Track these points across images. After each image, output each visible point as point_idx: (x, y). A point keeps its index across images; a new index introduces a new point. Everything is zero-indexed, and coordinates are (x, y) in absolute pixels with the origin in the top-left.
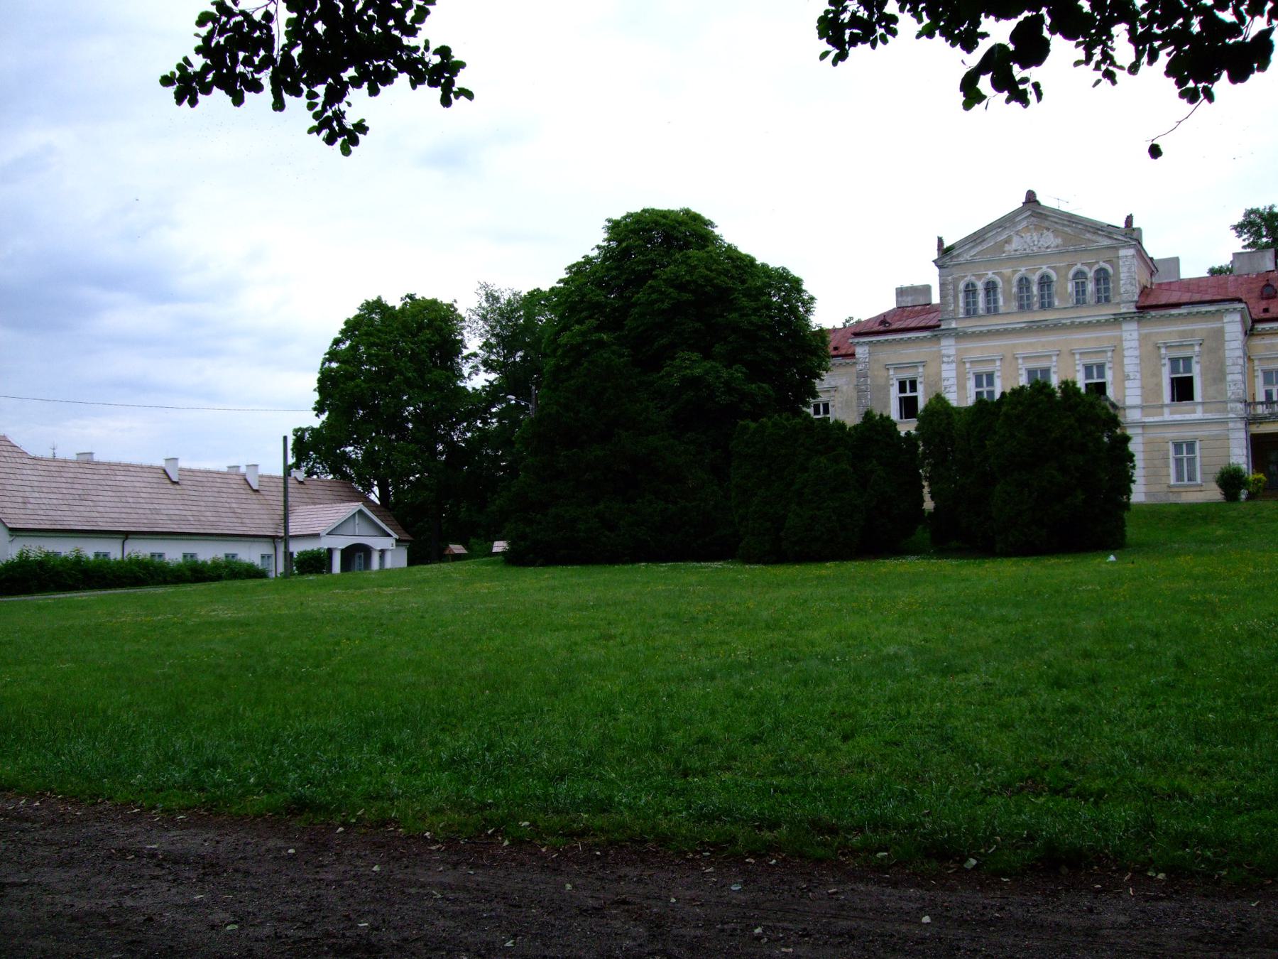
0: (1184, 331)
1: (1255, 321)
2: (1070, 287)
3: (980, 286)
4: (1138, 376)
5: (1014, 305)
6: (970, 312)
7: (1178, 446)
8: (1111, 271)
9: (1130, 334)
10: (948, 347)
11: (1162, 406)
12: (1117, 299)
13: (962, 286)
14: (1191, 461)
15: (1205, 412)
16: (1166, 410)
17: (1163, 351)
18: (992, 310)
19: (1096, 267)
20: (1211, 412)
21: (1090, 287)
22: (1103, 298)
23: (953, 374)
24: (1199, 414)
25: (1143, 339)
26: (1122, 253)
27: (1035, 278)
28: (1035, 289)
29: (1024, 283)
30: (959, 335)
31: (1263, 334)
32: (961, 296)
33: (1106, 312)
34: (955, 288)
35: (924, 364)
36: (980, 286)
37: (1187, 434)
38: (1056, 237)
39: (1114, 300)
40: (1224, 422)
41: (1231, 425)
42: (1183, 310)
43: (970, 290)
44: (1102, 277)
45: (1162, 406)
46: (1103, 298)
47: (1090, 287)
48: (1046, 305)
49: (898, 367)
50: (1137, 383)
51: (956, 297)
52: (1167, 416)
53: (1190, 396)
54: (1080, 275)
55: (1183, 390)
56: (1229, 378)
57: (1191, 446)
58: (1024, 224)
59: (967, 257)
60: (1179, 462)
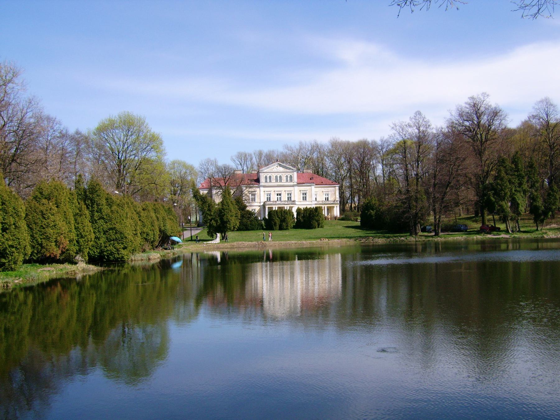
2: (285, 178)
6: (266, 181)
9: (297, 189)
10: (262, 189)
22: (291, 181)
24: (307, 203)
27: (279, 176)
30: (264, 186)
33: (292, 184)
42: (305, 184)
44: (291, 177)
46: (291, 181)
47: (289, 179)
48: (281, 181)
53: (306, 200)
54: (287, 176)
55: (305, 199)
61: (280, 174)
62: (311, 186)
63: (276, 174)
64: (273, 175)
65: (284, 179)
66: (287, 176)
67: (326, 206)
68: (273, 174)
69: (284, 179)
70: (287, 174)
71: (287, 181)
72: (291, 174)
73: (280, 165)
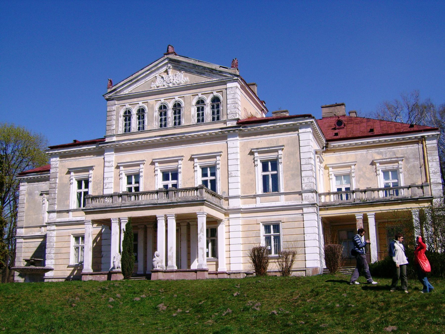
0: (271, 140)
1: (328, 141)
2: (194, 111)
3: (134, 112)
4: (239, 174)
5: (156, 125)
7: (267, 228)
8: (221, 99)
11: (255, 197)
12: (225, 118)
13: (122, 113)
14: (277, 238)
15: (286, 200)
16: (258, 199)
17: (256, 155)
18: (141, 129)
19: (211, 96)
20: (290, 200)
21: (208, 110)
23: (113, 174)
24: (282, 201)
25: (243, 146)
26: (229, 85)
27: (170, 105)
28: (170, 113)
29: (163, 109)
31: (334, 150)
32: (121, 119)
34: (118, 113)
35: (91, 168)
36: (134, 112)
37: (272, 217)
38: (185, 76)
39: (222, 119)
40: (299, 207)
41: (305, 210)
43: (128, 115)
45: (255, 197)
47: (208, 110)
49: (77, 170)
50: (239, 179)
51: (117, 120)
52: (259, 203)
56: (303, 174)
57: (277, 227)
58: (164, 69)
59: (126, 92)
60: (268, 239)
61: (177, 97)
62: (295, 129)
63: (162, 99)
64: (152, 106)
65: (190, 112)
66: (201, 102)
67: (371, 212)
68: (151, 100)
69: (190, 112)
70: (200, 93)
71: (201, 119)
72: (215, 91)
73: (178, 65)
